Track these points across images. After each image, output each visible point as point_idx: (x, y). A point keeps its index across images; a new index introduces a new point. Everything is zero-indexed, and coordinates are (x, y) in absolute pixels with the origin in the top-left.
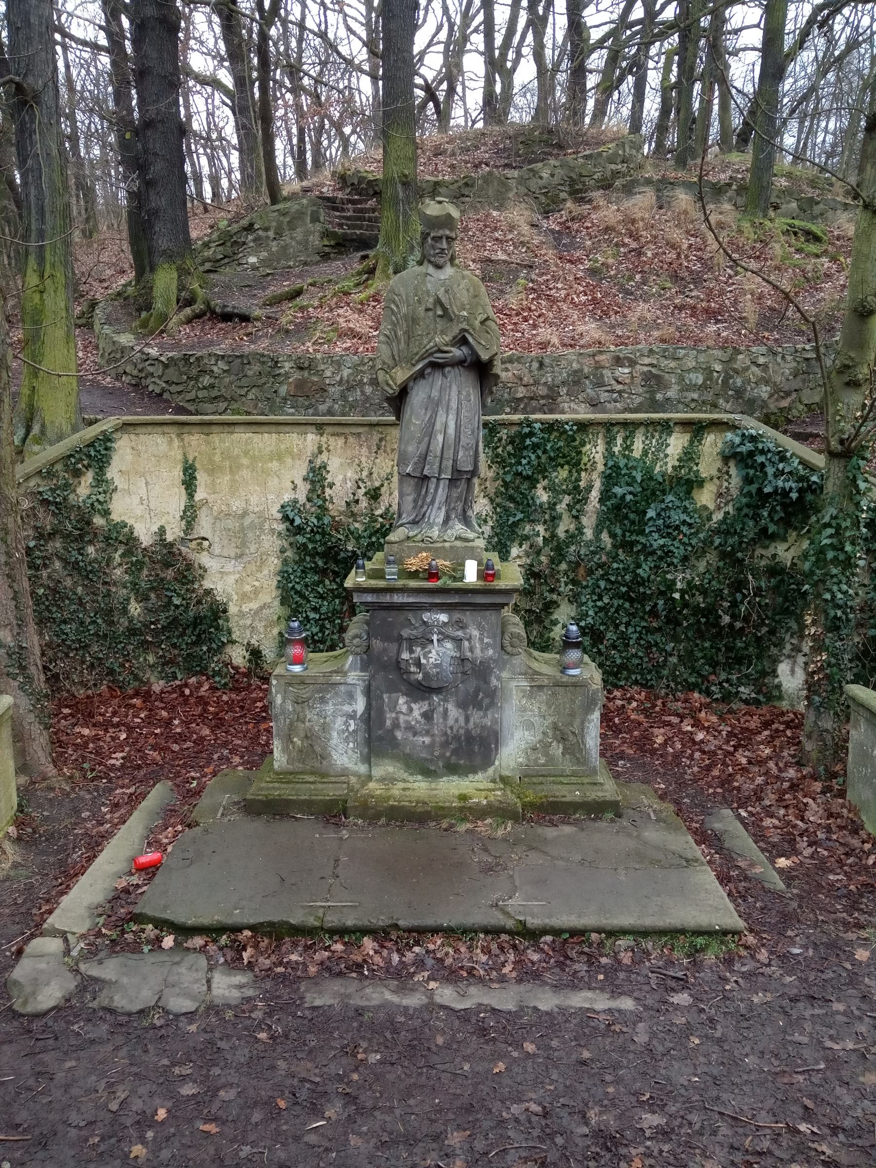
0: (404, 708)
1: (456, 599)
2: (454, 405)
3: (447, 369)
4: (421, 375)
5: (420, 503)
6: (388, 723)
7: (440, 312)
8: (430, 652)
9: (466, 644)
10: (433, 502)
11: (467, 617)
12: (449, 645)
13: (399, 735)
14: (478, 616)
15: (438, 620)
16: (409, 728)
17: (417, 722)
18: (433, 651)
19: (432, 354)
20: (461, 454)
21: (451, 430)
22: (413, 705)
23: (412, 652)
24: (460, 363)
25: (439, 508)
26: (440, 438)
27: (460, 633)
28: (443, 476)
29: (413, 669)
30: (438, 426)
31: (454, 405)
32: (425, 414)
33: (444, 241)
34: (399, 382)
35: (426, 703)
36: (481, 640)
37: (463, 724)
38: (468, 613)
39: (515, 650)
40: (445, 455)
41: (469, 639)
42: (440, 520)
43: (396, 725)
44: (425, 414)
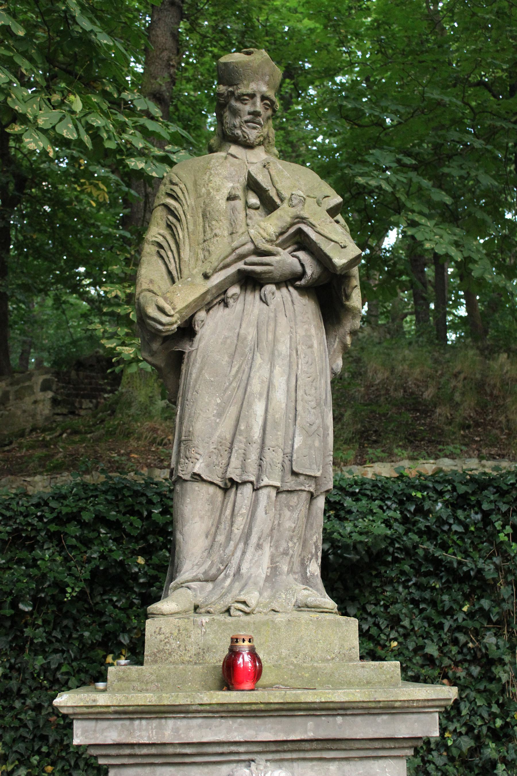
1: (308, 729)
2: (283, 348)
3: (270, 288)
4: (219, 298)
5: (221, 538)
7: (254, 200)
10: (247, 536)
19: (241, 257)
20: (298, 441)
21: (280, 396)
24: (290, 280)
25: (259, 546)
26: (259, 408)
28: (266, 481)
31: (283, 348)
32: (231, 364)
33: (258, 100)
34: (180, 305)
40: (270, 441)
42: (263, 570)
44: (231, 364)
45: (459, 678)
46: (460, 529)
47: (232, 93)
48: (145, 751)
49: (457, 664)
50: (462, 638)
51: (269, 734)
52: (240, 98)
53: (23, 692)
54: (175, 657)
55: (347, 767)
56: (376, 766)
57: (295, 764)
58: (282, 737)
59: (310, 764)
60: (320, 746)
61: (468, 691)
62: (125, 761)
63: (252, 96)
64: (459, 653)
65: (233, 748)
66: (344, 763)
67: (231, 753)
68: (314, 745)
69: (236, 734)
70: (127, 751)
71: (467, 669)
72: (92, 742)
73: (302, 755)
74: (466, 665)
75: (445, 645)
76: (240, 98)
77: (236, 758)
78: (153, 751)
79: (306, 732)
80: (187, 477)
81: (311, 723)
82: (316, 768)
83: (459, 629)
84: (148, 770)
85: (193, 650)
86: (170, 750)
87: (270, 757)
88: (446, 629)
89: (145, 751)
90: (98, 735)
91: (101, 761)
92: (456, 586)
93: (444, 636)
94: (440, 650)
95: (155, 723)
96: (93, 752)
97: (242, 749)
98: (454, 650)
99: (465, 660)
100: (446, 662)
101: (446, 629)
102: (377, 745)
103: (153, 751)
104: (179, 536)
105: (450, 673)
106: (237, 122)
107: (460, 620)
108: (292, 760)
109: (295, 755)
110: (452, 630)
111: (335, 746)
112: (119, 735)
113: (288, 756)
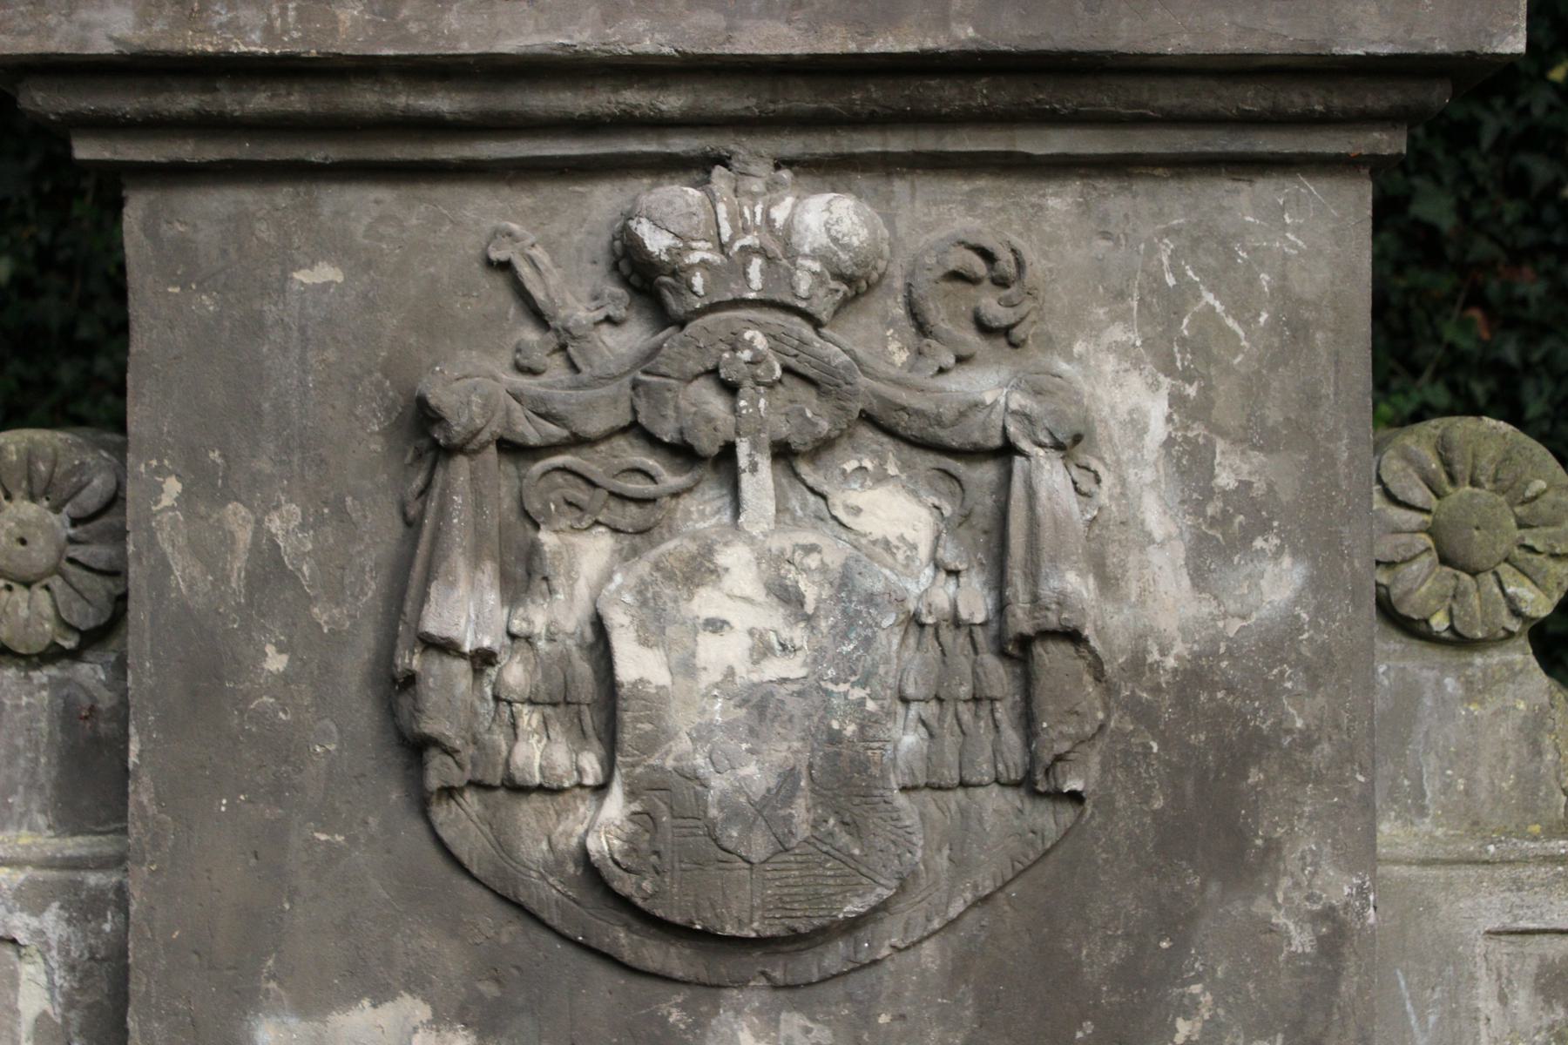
8: (699, 570)
9: (1050, 476)
11: (1051, 226)
12: (892, 512)
14: (1155, 225)
15: (780, 250)
18: (736, 559)
23: (524, 575)
27: (988, 389)
29: (538, 751)
36: (1189, 462)
38: (1059, 201)
39: (1480, 606)
41: (1069, 445)
45: (1524, 302)
48: (260, 101)
49: (1518, 256)
50: (1541, 170)
51: (784, 29)
53: (84, 332)
55: (1121, 202)
56: (1244, 204)
57: (900, 186)
58: (838, 42)
59: (963, 186)
60: (1005, 95)
61: (1549, 343)
62: (186, 150)
64: (1527, 221)
65: (634, 98)
66: (1107, 185)
67: (627, 123)
68: (982, 93)
69: (640, 24)
70: (187, 102)
71: (1549, 274)
72: (29, 46)
73: (927, 142)
74: (1549, 261)
75: (1480, 192)
77: (650, 146)
78: (296, 100)
79: (943, 21)
82: (988, 203)
83: (1532, 138)
84: (284, 196)
86: (366, 99)
87: (793, 145)
88: (1487, 140)
89: (260, 101)
90: (52, 19)
91: (85, 150)
93: (1477, 164)
94: (1463, 210)
96: (41, 100)
97: (672, 102)
98: (1512, 210)
99: (1547, 247)
100: (1482, 248)
101: (1487, 140)
102: (1252, 98)
103: (296, 100)
105: (1493, 288)
107: (1538, 111)
108: (887, 165)
109: (897, 143)
110: (1505, 144)
111: (1071, 97)
112: (144, 21)
113: (870, 143)
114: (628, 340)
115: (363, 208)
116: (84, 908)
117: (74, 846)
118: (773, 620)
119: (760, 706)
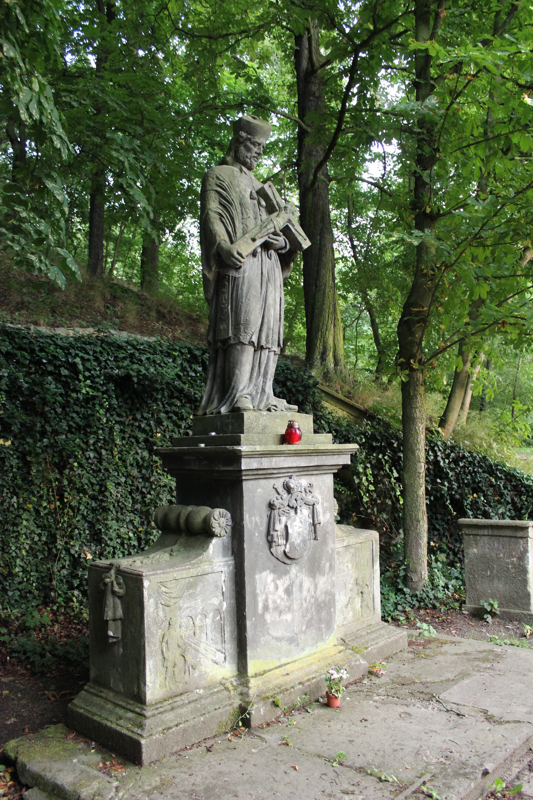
0: (272, 587)
6: (260, 605)
11: (313, 479)
13: (268, 617)
16: (276, 608)
17: (282, 599)
22: (278, 582)
30: (270, 301)
35: (287, 577)
37: (313, 594)
43: (266, 608)
46: (193, 374)
47: (250, 139)
52: (254, 144)
54: (255, 430)
63: (259, 144)
76: (254, 144)
80: (247, 343)
81: (316, 458)
84: (256, 481)
85: (261, 427)
92: (188, 405)
95: (269, 459)
104: (237, 372)
106: (249, 155)
114: (285, 495)
115: (262, 482)
116: (229, 566)
117: (226, 559)
118: (300, 524)
119: (299, 534)
